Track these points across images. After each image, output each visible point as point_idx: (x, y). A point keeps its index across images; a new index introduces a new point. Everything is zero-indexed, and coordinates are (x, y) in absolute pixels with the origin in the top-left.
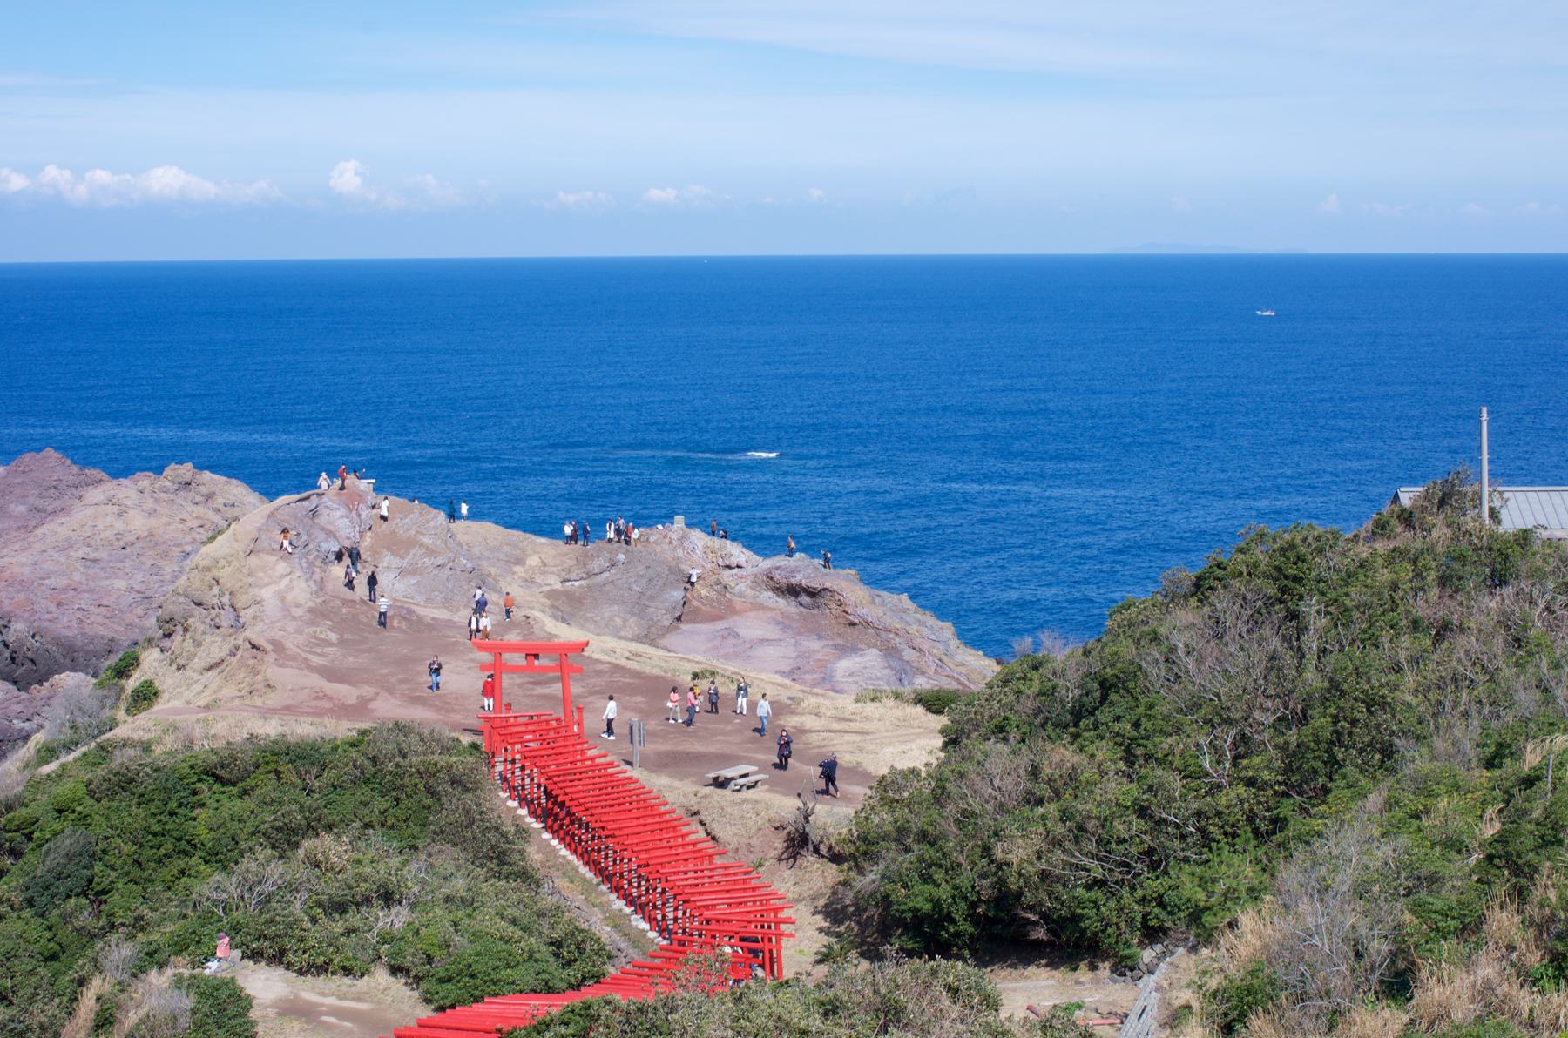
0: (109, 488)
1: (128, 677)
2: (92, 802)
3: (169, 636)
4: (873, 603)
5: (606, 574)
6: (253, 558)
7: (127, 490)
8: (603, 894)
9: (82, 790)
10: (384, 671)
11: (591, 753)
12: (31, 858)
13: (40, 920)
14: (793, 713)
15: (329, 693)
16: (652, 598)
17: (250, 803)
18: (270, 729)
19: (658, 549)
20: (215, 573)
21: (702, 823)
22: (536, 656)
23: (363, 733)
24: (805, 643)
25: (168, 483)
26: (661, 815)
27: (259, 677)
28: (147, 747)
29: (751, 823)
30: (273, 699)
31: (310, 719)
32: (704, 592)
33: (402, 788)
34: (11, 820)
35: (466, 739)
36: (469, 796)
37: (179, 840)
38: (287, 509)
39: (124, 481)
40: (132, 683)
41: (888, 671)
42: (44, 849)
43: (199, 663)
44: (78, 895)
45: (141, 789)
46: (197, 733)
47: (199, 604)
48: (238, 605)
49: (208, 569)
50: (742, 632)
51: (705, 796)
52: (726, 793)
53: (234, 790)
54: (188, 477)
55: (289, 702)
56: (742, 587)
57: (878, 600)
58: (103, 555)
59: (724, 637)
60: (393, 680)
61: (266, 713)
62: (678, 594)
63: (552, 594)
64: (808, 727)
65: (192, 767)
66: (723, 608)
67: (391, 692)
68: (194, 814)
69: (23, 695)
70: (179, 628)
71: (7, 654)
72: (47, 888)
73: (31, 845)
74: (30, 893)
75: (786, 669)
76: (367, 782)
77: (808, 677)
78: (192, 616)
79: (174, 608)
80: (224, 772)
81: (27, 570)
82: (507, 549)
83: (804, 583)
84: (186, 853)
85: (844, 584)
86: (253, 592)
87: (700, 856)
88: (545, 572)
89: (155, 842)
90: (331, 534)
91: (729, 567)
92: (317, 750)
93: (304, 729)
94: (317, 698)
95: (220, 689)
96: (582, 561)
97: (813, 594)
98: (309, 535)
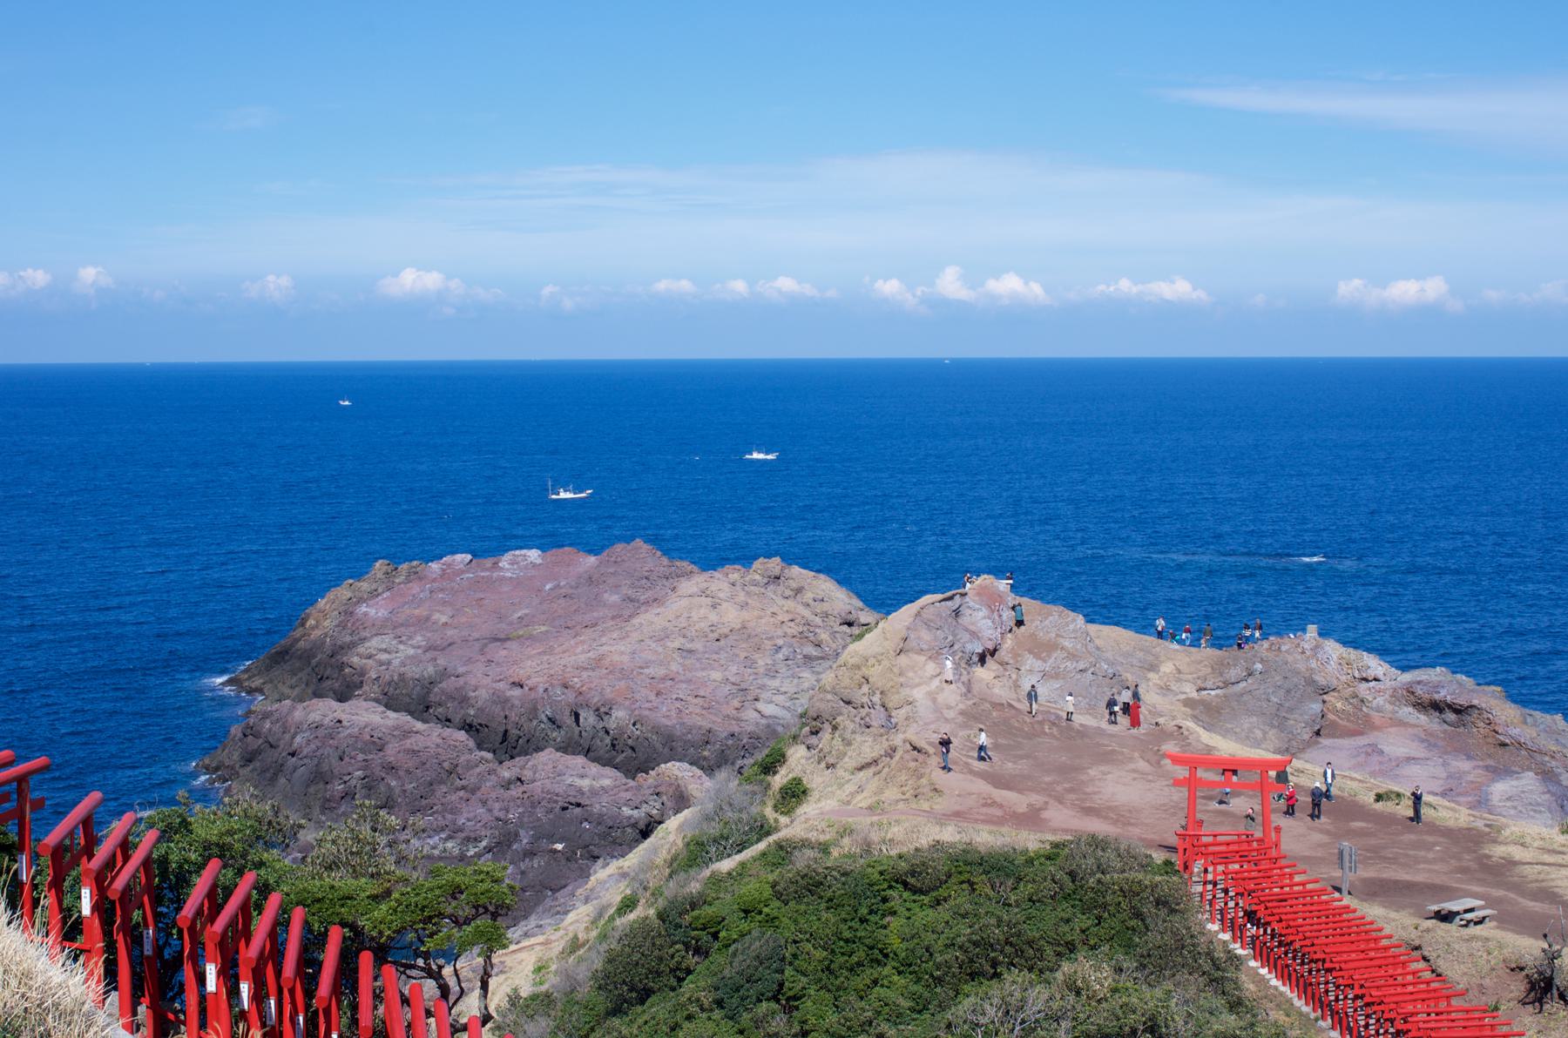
0: (695, 583)
1: (775, 773)
2: (777, 903)
3: (817, 733)
4: (1525, 722)
5: (1243, 684)
6: (903, 660)
7: (721, 582)
8: (1321, 1030)
9: (768, 892)
10: (1047, 779)
11: (1297, 879)
12: (718, 958)
13: (731, 1023)
14: (1495, 841)
15: (998, 800)
16: (1290, 710)
17: (943, 913)
18: (949, 834)
19: (1290, 658)
20: (865, 671)
21: (1425, 959)
22: (1235, 772)
23: (1056, 845)
24: (1454, 763)
25: (757, 577)
26: (1386, 948)
27: (924, 781)
28: (824, 848)
29: (1482, 962)
30: (941, 805)
31: (987, 827)
32: (1339, 705)
33: (1105, 906)
34: (697, 918)
35: (1159, 857)
36: (1177, 918)
37: (871, 948)
38: (932, 609)
39: (716, 574)
40: (779, 780)
41: (1547, 796)
42: (733, 947)
43: (849, 762)
44: (768, 1000)
45: (829, 894)
46: (875, 837)
47: (848, 703)
48: (890, 705)
49: (858, 667)
50: (1386, 749)
51: (1428, 930)
52: (1452, 929)
53: (926, 899)
54: (777, 571)
55: (957, 808)
56: (1380, 701)
57: (1529, 720)
58: (698, 645)
59: (1368, 754)
60: (1059, 788)
61: (942, 819)
62: (1316, 707)
63: (1189, 703)
64: (1517, 858)
65: (881, 873)
66: (1360, 724)
67: (1060, 800)
68: (885, 921)
69: (631, 783)
70: (827, 726)
71: (608, 740)
72: (738, 990)
73: (717, 945)
74: (720, 994)
75: (1439, 790)
76: (1067, 897)
77: (1462, 799)
78: (841, 714)
79: (825, 705)
80: (916, 879)
81: (626, 659)
82: (1140, 655)
83: (1449, 699)
84: (878, 962)
85: (1493, 702)
86: (905, 692)
87: (1436, 996)
88: (1179, 680)
89: (847, 949)
90: (974, 635)
91: (1366, 680)
92: (1012, 862)
93: (986, 838)
94: (985, 805)
95: (880, 791)
96: (1219, 668)
97: (1459, 710)
98: (955, 635)
